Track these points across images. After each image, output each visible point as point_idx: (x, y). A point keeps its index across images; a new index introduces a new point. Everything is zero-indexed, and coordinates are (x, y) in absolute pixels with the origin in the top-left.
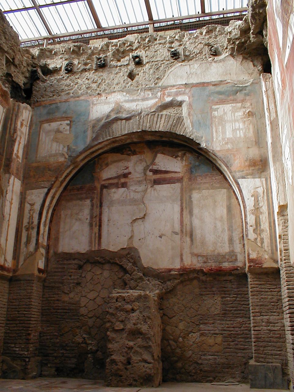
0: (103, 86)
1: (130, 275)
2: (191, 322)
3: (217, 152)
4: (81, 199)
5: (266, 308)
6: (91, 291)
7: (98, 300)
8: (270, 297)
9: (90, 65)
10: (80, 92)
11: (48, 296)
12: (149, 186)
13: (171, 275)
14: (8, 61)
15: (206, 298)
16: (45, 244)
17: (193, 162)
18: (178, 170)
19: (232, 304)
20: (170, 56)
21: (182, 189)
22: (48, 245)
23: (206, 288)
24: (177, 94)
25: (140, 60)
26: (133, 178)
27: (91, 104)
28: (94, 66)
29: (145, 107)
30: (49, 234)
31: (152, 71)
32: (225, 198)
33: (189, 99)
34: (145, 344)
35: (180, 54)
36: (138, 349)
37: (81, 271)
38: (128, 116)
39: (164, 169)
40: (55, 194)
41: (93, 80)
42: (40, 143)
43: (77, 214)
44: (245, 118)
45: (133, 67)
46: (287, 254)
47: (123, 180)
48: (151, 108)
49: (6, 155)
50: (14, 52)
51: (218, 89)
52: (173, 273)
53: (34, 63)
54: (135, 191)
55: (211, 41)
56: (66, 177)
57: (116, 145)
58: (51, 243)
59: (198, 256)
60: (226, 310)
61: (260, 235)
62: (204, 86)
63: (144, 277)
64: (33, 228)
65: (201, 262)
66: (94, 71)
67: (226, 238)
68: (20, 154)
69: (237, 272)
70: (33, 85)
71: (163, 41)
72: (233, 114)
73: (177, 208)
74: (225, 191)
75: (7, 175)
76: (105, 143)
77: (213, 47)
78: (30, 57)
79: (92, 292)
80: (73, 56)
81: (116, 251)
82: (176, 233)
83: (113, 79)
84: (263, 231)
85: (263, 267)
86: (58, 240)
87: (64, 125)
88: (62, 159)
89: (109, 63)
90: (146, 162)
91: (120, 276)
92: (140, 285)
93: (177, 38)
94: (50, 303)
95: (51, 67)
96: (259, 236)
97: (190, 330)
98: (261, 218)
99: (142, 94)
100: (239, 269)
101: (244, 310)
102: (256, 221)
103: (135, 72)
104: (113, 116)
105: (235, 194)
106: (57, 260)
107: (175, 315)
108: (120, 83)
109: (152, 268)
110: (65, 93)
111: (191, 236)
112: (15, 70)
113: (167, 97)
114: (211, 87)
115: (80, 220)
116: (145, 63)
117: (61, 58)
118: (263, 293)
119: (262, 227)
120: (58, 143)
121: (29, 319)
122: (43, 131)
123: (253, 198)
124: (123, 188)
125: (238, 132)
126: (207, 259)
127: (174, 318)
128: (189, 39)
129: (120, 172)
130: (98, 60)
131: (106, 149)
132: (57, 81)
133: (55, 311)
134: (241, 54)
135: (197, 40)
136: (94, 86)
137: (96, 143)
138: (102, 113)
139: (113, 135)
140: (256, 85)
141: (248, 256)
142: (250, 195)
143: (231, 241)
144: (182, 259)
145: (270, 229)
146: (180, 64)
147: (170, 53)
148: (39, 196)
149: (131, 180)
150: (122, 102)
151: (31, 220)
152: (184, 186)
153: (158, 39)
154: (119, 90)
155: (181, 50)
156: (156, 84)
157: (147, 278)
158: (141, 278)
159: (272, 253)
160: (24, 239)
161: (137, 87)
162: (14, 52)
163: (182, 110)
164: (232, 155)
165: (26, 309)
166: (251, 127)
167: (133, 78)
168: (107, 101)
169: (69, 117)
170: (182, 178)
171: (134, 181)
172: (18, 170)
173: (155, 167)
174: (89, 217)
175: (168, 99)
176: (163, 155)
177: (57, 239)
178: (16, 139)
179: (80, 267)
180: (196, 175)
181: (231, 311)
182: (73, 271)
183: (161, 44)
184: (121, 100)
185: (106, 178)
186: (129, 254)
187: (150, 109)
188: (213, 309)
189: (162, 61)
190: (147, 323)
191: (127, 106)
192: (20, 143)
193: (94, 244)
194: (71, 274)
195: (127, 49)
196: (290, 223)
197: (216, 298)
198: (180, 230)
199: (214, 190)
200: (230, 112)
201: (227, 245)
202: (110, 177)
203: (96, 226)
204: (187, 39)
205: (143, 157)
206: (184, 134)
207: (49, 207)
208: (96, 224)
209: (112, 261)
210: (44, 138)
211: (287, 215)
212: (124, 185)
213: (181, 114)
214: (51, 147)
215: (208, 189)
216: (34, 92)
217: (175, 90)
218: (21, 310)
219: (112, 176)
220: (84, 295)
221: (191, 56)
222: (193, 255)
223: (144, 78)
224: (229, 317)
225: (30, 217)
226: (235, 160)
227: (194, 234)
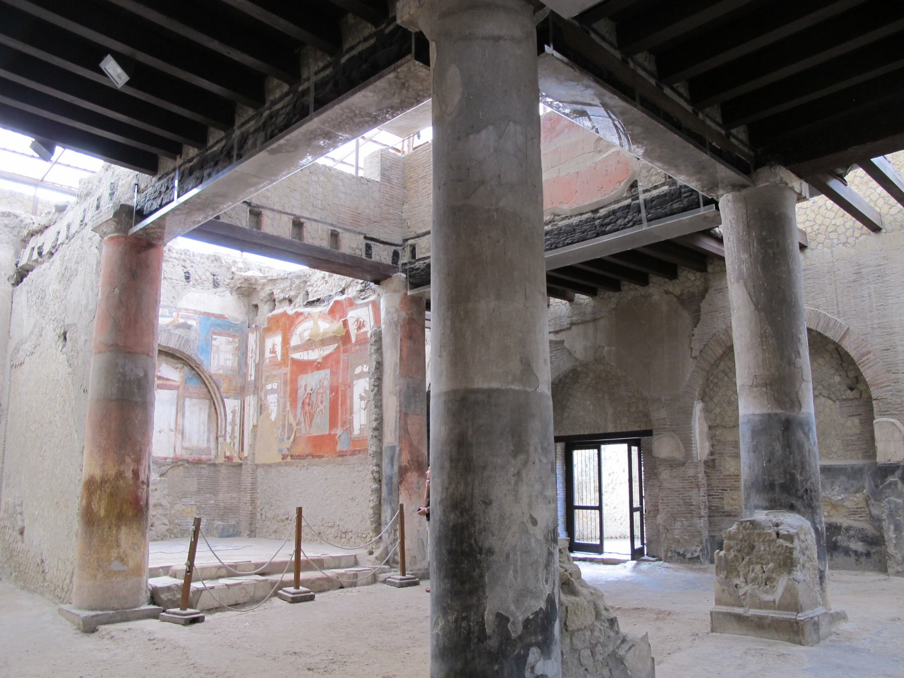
17: (188, 375)
21: (178, 396)
23: (188, 472)
24: (188, 318)
34: (164, 513)
36: (159, 516)
48: (167, 325)
51: (218, 322)
59: (186, 449)
69: (209, 462)
74: (208, 401)
82: (172, 430)
97: (176, 502)
111: (183, 434)
141: (225, 453)
142: (230, 411)
144: (175, 451)
146: (192, 289)
155: (191, 271)
166: (237, 358)
175: (181, 321)
187: (167, 327)
201: (206, 443)
215: (195, 398)
222: (183, 448)
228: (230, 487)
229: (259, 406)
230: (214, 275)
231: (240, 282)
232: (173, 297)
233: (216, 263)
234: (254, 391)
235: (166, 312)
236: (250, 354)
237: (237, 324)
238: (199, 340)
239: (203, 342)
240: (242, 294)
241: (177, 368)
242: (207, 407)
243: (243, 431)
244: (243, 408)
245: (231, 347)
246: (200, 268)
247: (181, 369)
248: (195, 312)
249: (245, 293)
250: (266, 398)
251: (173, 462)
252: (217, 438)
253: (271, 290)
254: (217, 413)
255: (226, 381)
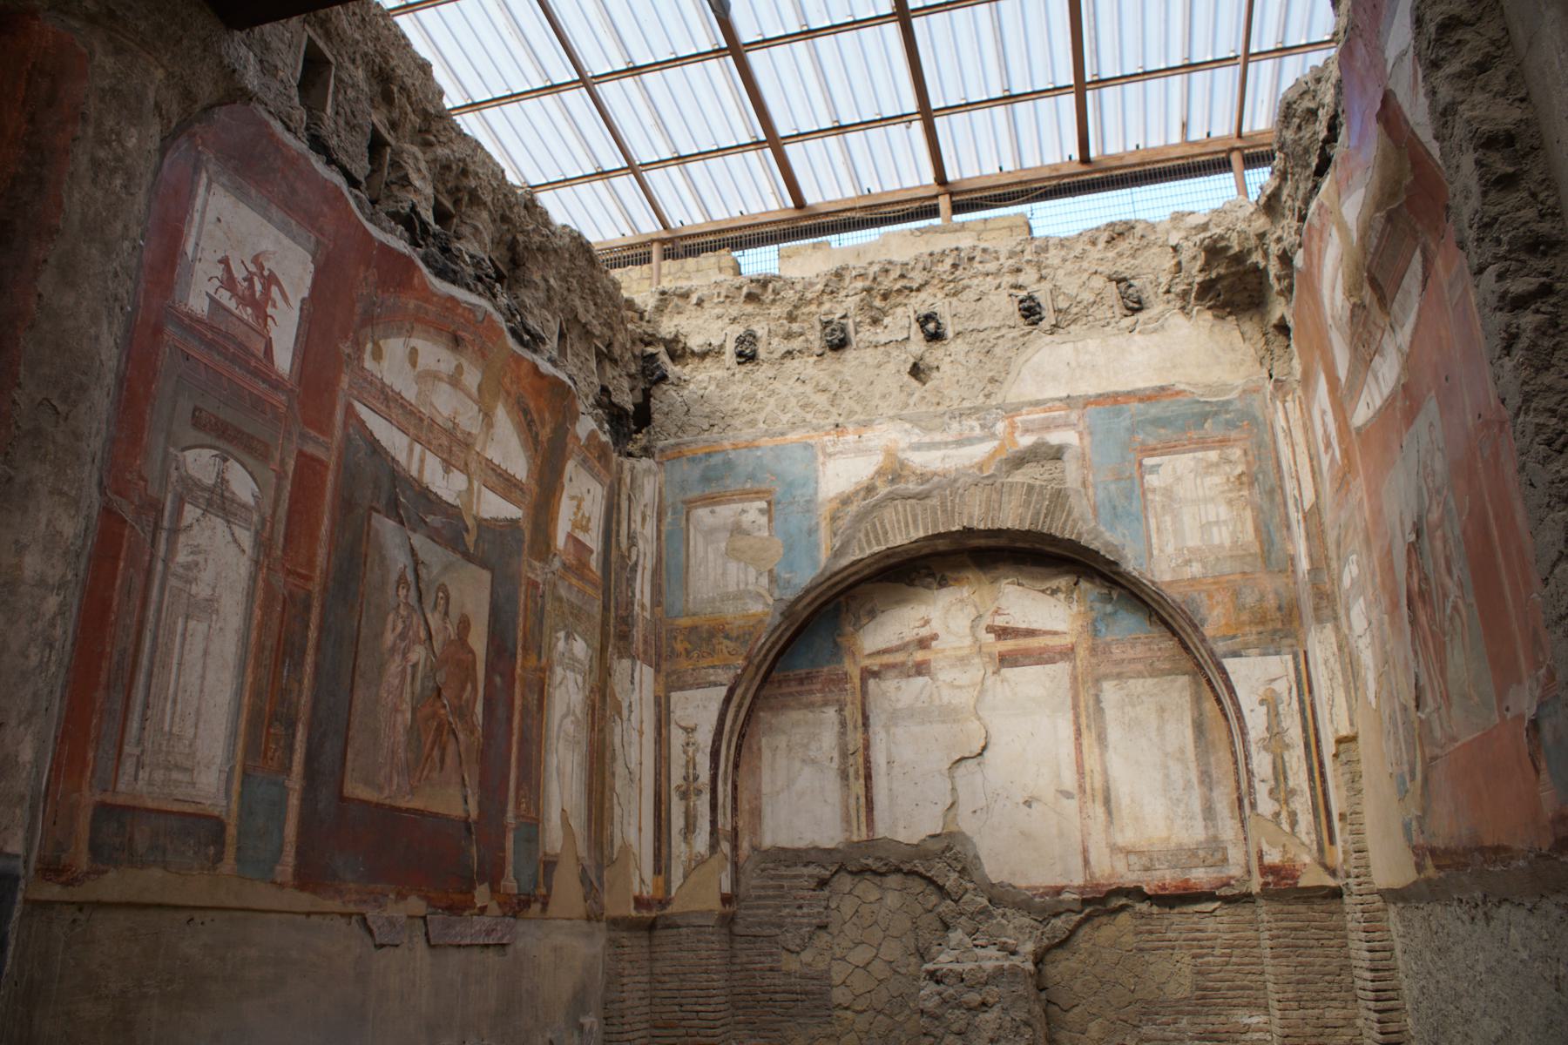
0: (847, 403)
1: (956, 902)
2: (1119, 1019)
3: (1163, 588)
4: (810, 706)
5: (1312, 987)
6: (857, 944)
7: (878, 968)
8: (1322, 960)
9: (802, 338)
10: (785, 418)
11: (745, 959)
12: (990, 671)
13: (1060, 902)
14: (599, 354)
15: (1152, 959)
16: (729, 828)
17: (1097, 605)
18: (1061, 627)
19: (1220, 971)
20: (1017, 314)
21: (1074, 679)
22: (735, 829)
23: (1151, 932)
24: (1047, 426)
25: (938, 325)
26: (944, 650)
27: (820, 453)
28: (817, 346)
29: (967, 463)
30: (735, 799)
31: (974, 358)
32: (1188, 698)
33: (1081, 439)
35: (1043, 305)
37: (826, 893)
38: (921, 488)
39: (1023, 626)
40: (743, 697)
41: (817, 385)
42: (692, 561)
43: (806, 746)
44: (1230, 491)
45: (924, 348)
46: (1363, 862)
47: (919, 656)
49: (616, 609)
50: (612, 329)
51: (1154, 410)
52: (1066, 896)
53: (646, 333)
54: (952, 686)
55: (1123, 267)
56: (769, 651)
57: (892, 561)
58: (741, 824)
59: (1128, 853)
60: (1206, 989)
61: (1287, 803)
62: (1116, 402)
63: (991, 908)
64: (699, 792)
65: (1137, 867)
66: (815, 358)
67: (1196, 806)
68: (647, 601)
70: (651, 396)
71: (992, 266)
72: (1199, 481)
73: (1066, 729)
74: (1184, 680)
75: (626, 663)
76: (867, 561)
77: (1130, 286)
78: (637, 316)
79: (860, 949)
80: (749, 308)
81: (915, 842)
82: (1068, 795)
83: (872, 383)
84: (1292, 792)
85: (1300, 885)
86: (760, 816)
87: (752, 513)
88: (756, 608)
89: (852, 334)
90: (976, 606)
91: (929, 906)
92: (983, 928)
93: (1027, 256)
94: (754, 977)
95: (695, 343)
96: (1284, 807)
98: (1286, 758)
99: (955, 425)
100: (1233, 882)
101: (1251, 989)
102: (1274, 767)
103: (930, 360)
104: (883, 490)
105: (1213, 689)
106: (763, 866)
107: (1076, 1002)
108: (890, 394)
109: (1010, 885)
110: (744, 420)
111: (1107, 801)
112: (616, 374)
113: (1022, 436)
114: (1136, 404)
115: (813, 761)
116: (950, 333)
117: (718, 317)
118: (1302, 950)
119: (1291, 784)
120: (742, 564)
121: (711, 1024)
122: (695, 528)
123: (1264, 709)
124: (920, 678)
125: (1215, 529)
126: (1151, 860)
127: (1076, 1010)
128: (1064, 260)
129: (910, 634)
130: (825, 328)
131: (866, 572)
132: (717, 386)
133: (767, 997)
134: (1209, 308)
135: (1085, 265)
136: (822, 400)
137: (844, 562)
138: (854, 480)
139: (887, 541)
140: (1255, 395)
141: (1261, 857)
142: (1256, 699)
143: (1209, 812)
144: (1086, 862)
145: (1312, 789)
147: (1016, 304)
148: (705, 707)
149: (940, 655)
150: (903, 450)
151: (691, 771)
152: (1079, 670)
153: (977, 259)
154: (891, 413)
155: (1043, 297)
156: (987, 396)
157: (1000, 911)
158: (983, 911)
159: (1321, 850)
160: (678, 822)
161: (938, 404)
162: (612, 329)
163: (1063, 472)
164: (1203, 595)
165: (701, 1000)
166: (1248, 514)
167: (922, 376)
168: (861, 445)
169: (764, 492)
170: (1072, 649)
171: (946, 657)
172: (645, 642)
173: (1000, 621)
174: (836, 755)
175: (1026, 441)
176: (1020, 588)
177: (756, 813)
178: (636, 564)
179: (823, 883)
180: (1109, 639)
181: (1219, 989)
182: (805, 893)
183: (988, 275)
184: (902, 445)
185: (874, 649)
186: (949, 848)
187: (981, 469)
188: (1172, 986)
189: (998, 328)
190: (1022, 1036)
191: (917, 459)
192: (644, 568)
193: (855, 824)
194: (802, 901)
195: (898, 286)
196: (1364, 783)
197: (1178, 958)
198: (1076, 785)
199: (1156, 680)
200: (1192, 475)
201: (1199, 823)
202: (883, 646)
203: (857, 778)
204: (1056, 262)
205: (965, 592)
206: (1073, 537)
207: (732, 732)
208: (857, 772)
209: (906, 867)
210: (701, 548)
211: (1359, 761)
212: (921, 669)
213: (1063, 481)
214: (724, 574)
215: (1140, 675)
216: (656, 416)
217: (1043, 415)
218: (688, 1000)
219: (888, 645)
220: (838, 956)
221: (1074, 310)
222: (1114, 849)
223: (956, 379)
224: (1216, 1005)
225: (688, 762)
226: (1211, 608)
227: (1113, 796)
228: (1304, 982)
229: (1347, 660)
230: (1119, 281)
231: (1197, 268)
232: (992, 380)
233: (1123, 245)
234: (1316, 609)
235: (972, 429)
236: (1290, 486)
237: (1229, 402)
238: (1095, 487)
239: (1113, 487)
240: (1223, 306)
241: (1054, 592)
242: (1186, 699)
243: (1321, 764)
244: (1304, 684)
245: (1217, 479)
246: (1070, 274)
247: (1070, 592)
248: (1069, 401)
249: (1238, 298)
250: (1350, 627)
251: (1086, 902)
252: (1240, 800)
253: (1279, 240)
254: (1225, 716)
255: (1218, 598)
